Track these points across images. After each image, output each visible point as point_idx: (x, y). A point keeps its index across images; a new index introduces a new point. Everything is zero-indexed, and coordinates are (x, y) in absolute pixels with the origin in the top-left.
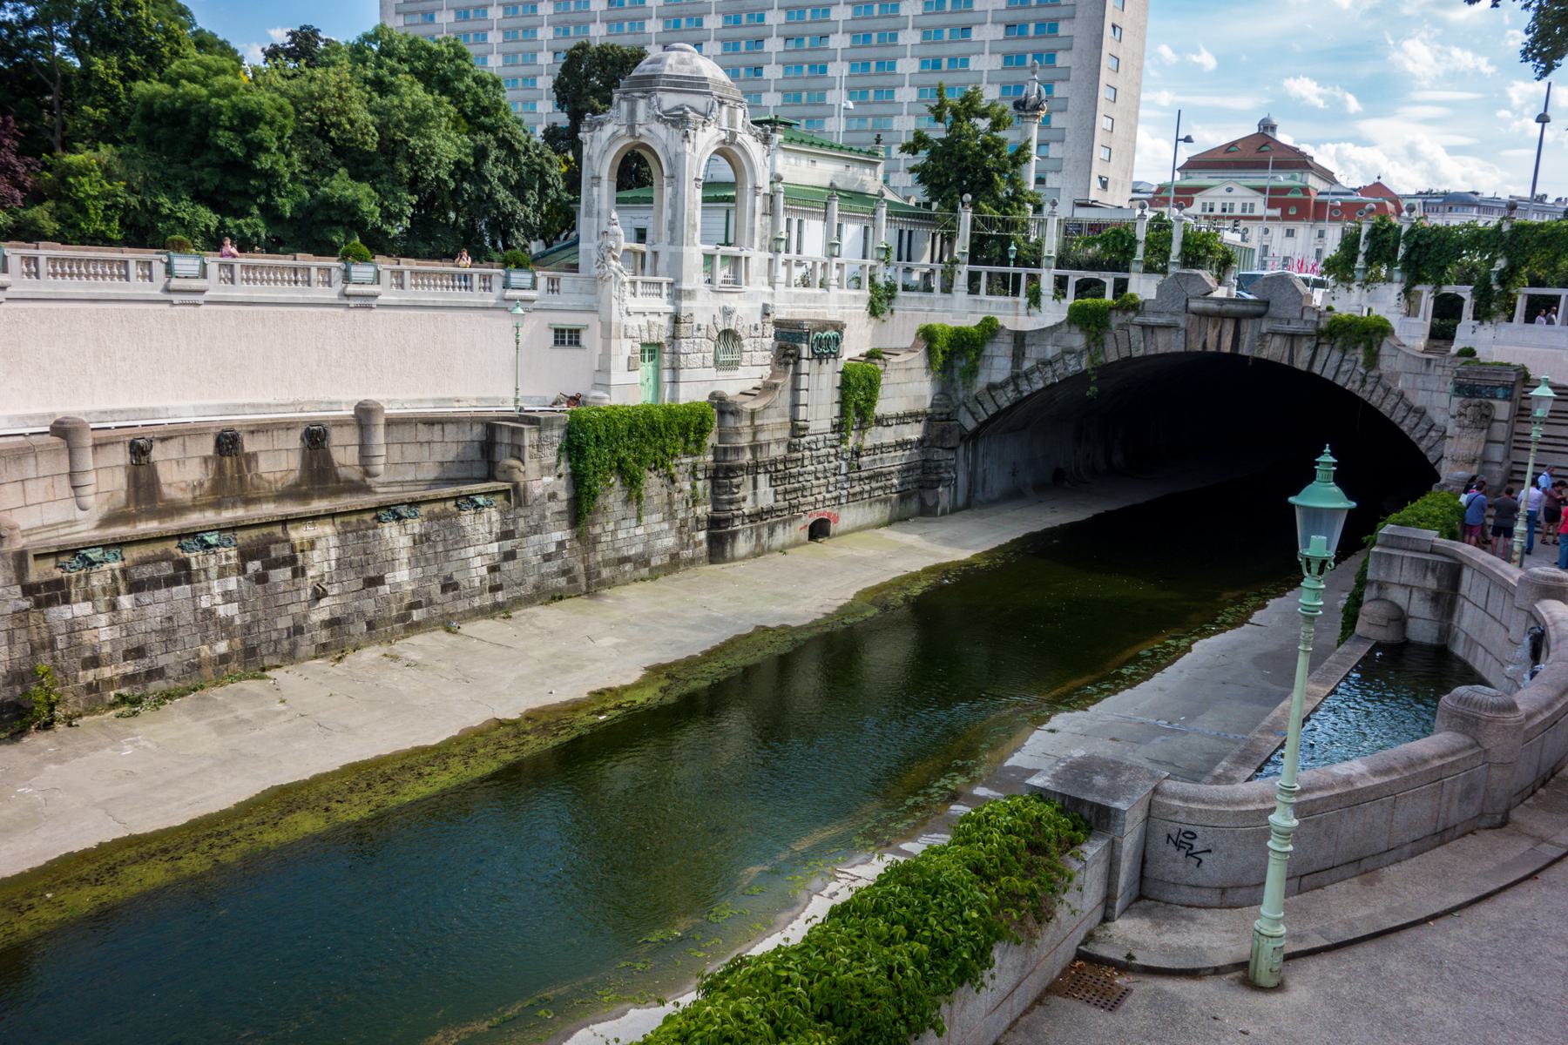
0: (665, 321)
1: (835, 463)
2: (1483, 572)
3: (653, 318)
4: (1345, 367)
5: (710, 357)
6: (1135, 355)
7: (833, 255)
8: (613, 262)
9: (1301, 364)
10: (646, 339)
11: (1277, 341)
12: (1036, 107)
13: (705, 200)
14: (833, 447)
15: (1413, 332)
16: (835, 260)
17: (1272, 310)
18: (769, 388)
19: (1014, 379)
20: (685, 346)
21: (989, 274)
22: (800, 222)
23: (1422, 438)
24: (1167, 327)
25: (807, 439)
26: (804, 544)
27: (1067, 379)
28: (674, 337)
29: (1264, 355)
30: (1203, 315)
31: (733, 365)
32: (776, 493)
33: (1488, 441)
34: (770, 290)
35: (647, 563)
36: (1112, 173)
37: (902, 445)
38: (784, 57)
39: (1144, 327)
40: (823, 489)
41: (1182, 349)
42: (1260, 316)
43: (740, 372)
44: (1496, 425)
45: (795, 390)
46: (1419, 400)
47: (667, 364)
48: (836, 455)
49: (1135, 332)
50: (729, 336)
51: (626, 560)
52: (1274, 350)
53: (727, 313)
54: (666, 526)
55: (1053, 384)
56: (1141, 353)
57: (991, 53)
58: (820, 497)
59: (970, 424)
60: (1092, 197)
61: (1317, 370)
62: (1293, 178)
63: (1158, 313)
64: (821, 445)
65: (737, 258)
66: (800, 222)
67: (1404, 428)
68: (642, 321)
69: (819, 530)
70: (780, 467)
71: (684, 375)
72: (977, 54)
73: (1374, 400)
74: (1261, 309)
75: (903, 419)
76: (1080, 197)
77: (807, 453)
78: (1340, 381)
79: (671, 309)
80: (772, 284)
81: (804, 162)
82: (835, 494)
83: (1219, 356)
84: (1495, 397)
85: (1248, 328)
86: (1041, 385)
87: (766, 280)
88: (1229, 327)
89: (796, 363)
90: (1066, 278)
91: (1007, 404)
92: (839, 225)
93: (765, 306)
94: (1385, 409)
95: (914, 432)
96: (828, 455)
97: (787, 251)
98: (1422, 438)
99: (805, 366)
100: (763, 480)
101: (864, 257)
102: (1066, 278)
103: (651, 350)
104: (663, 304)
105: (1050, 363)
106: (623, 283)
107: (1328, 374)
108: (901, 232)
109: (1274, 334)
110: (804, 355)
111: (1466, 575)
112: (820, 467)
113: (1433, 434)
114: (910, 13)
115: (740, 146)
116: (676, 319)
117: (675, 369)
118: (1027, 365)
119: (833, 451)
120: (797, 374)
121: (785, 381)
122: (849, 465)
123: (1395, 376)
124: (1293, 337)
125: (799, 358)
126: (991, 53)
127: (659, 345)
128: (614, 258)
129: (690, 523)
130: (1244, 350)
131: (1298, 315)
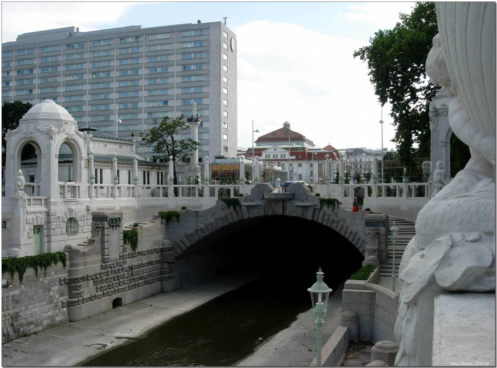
0: (43, 216)
1: (122, 273)
2: (383, 294)
3: (38, 215)
4: (325, 218)
5: (64, 229)
6: (245, 218)
7: (116, 184)
8: (20, 191)
9: (309, 218)
10: (35, 224)
11: (299, 208)
12: (196, 120)
13: (59, 162)
14: (121, 266)
15: (348, 203)
16: (118, 185)
17: (296, 197)
18: (91, 242)
20: (53, 225)
21: (183, 188)
22: (101, 170)
23: (357, 243)
24: (257, 206)
25: (109, 263)
26: (110, 310)
27: (219, 229)
28: (48, 222)
29: (295, 215)
30: (270, 201)
31: (75, 233)
32: (97, 288)
33: (379, 243)
34: (89, 199)
35: (41, 324)
36: (229, 145)
37: (150, 263)
38: (91, 102)
39: (247, 207)
40: (118, 285)
41: (263, 214)
42: (292, 199)
43: (78, 236)
44: (381, 236)
45: (103, 242)
47: (45, 234)
48: (123, 270)
50: (72, 221)
51: (32, 323)
52: (298, 213)
53: (71, 211)
54: (48, 306)
55: (212, 233)
56: (247, 217)
57: (177, 99)
58: (116, 289)
60: (222, 155)
61: (315, 219)
62: (299, 144)
63: (253, 201)
64: (115, 265)
65: (75, 187)
66: (101, 170)
67: (350, 240)
68: (34, 216)
69: (117, 303)
70: (98, 276)
71: (53, 238)
73: (338, 230)
74: (292, 197)
75: (150, 252)
76: (217, 155)
77: (109, 269)
78: (325, 223)
79: (46, 210)
80: (90, 197)
81: (102, 145)
82: (123, 286)
84: (379, 226)
85: (289, 205)
86: (207, 233)
87: (87, 196)
88: (281, 204)
89: (103, 231)
91: (194, 242)
92: (118, 171)
93: (87, 206)
94: (342, 233)
95: (155, 257)
96: (119, 270)
97: (96, 182)
98: (357, 243)
99: (106, 232)
100: (91, 282)
101: (129, 183)
103: (38, 229)
104: (43, 208)
106: (25, 200)
107: (320, 221)
108: (144, 172)
109: (298, 206)
110: (106, 227)
111: (377, 296)
112: (116, 275)
113: (360, 241)
114: (142, 84)
115: (74, 140)
116: (48, 214)
117: (49, 236)
118: (202, 226)
119: (121, 268)
120: (103, 235)
121: (98, 239)
122: (128, 274)
123: (344, 220)
125: (104, 228)
126: (177, 99)
127: (42, 226)
128: (21, 189)
129: (60, 304)
130: (288, 213)
131: (306, 198)
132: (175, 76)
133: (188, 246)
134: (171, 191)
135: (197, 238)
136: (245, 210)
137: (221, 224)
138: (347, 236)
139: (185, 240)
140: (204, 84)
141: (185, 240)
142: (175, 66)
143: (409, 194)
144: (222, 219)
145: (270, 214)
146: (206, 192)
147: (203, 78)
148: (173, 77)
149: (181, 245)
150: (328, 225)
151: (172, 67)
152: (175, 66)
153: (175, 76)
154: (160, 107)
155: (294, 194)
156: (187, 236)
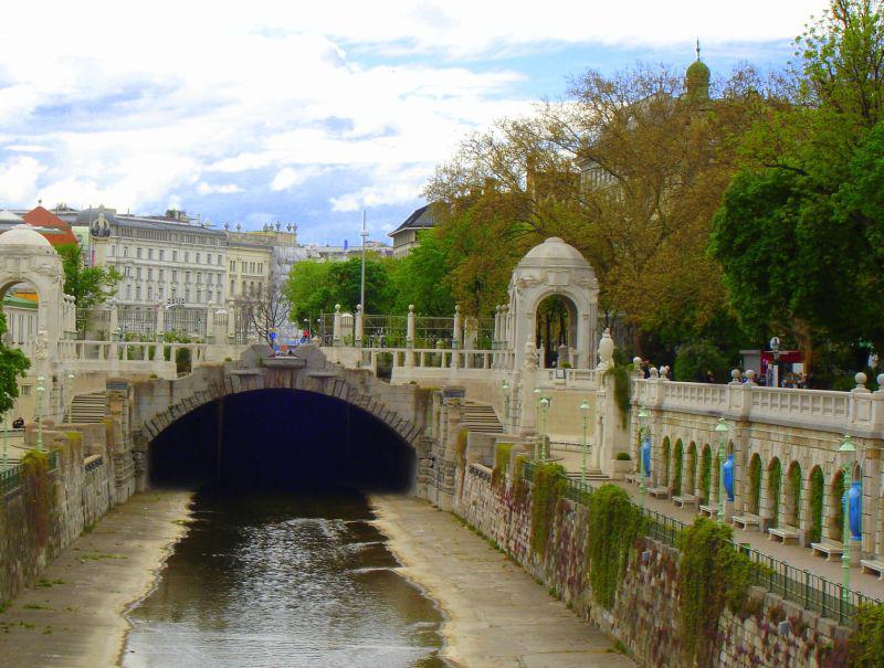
6: (236, 392)
19: (171, 408)
24: (254, 375)
29: (308, 388)
30: (274, 368)
39: (240, 376)
41: (262, 387)
42: (301, 368)
46: (391, 406)
49: (236, 381)
59: (151, 439)
73: (369, 409)
83: (284, 391)
86: (184, 413)
90: (170, 347)
94: (375, 413)
102: (170, 347)
105: (189, 399)
109: (313, 377)
118: (176, 401)
124: (323, 379)
130: (298, 386)
133: (161, 430)
138: (382, 416)
143: (417, 363)
145: (271, 387)
146: (160, 352)
150: (355, 403)
155: (306, 361)
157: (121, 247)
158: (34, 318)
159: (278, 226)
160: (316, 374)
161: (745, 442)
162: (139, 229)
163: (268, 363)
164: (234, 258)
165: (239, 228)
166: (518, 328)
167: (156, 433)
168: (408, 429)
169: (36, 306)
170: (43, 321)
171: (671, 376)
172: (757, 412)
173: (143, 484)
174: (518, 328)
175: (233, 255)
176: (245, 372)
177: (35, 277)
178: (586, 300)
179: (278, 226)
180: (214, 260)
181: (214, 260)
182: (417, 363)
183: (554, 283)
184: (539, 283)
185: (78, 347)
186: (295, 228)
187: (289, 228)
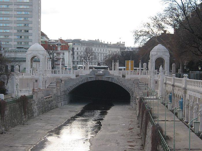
29: (105, 80)
49: (89, 78)
61: (112, 81)
63: (91, 75)
72: (11, 23)
73: (120, 85)
78: (115, 83)
94: (121, 85)
123: (121, 82)
132: (13, 11)
134: (61, 72)
135: (74, 88)
136: (89, 78)
137: (81, 83)
139: (70, 88)
140: (29, 16)
141: (70, 88)
142: (13, 5)
144: (81, 81)
147: (29, 13)
148: (12, 11)
149: (69, 89)
151: (11, 6)
152: (13, 5)
153: (13, 11)
154: (4, 26)
156: (70, 87)
157: (82, 48)
158: (38, 64)
159: (120, 42)
160: (107, 77)
161: (173, 90)
162: (86, 43)
163: (96, 74)
164: (109, 50)
165: (111, 43)
166: (152, 64)
167: (70, 91)
168: (129, 90)
169: (40, 61)
170: (41, 65)
171: (189, 77)
172: (176, 84)
173: (67, 102)
174: (152, 64)
175: (109, 49)
176: (91, 76)
177: (39, 55)
178: (167, 58)
179: (120, 42)
180: (105, 50)
181: (105, 50)
182: (131, 74)
183: (160, 55)
184: (156, 55)
185: (52, 71)
186: (124, 43)
187: (123, 43)
